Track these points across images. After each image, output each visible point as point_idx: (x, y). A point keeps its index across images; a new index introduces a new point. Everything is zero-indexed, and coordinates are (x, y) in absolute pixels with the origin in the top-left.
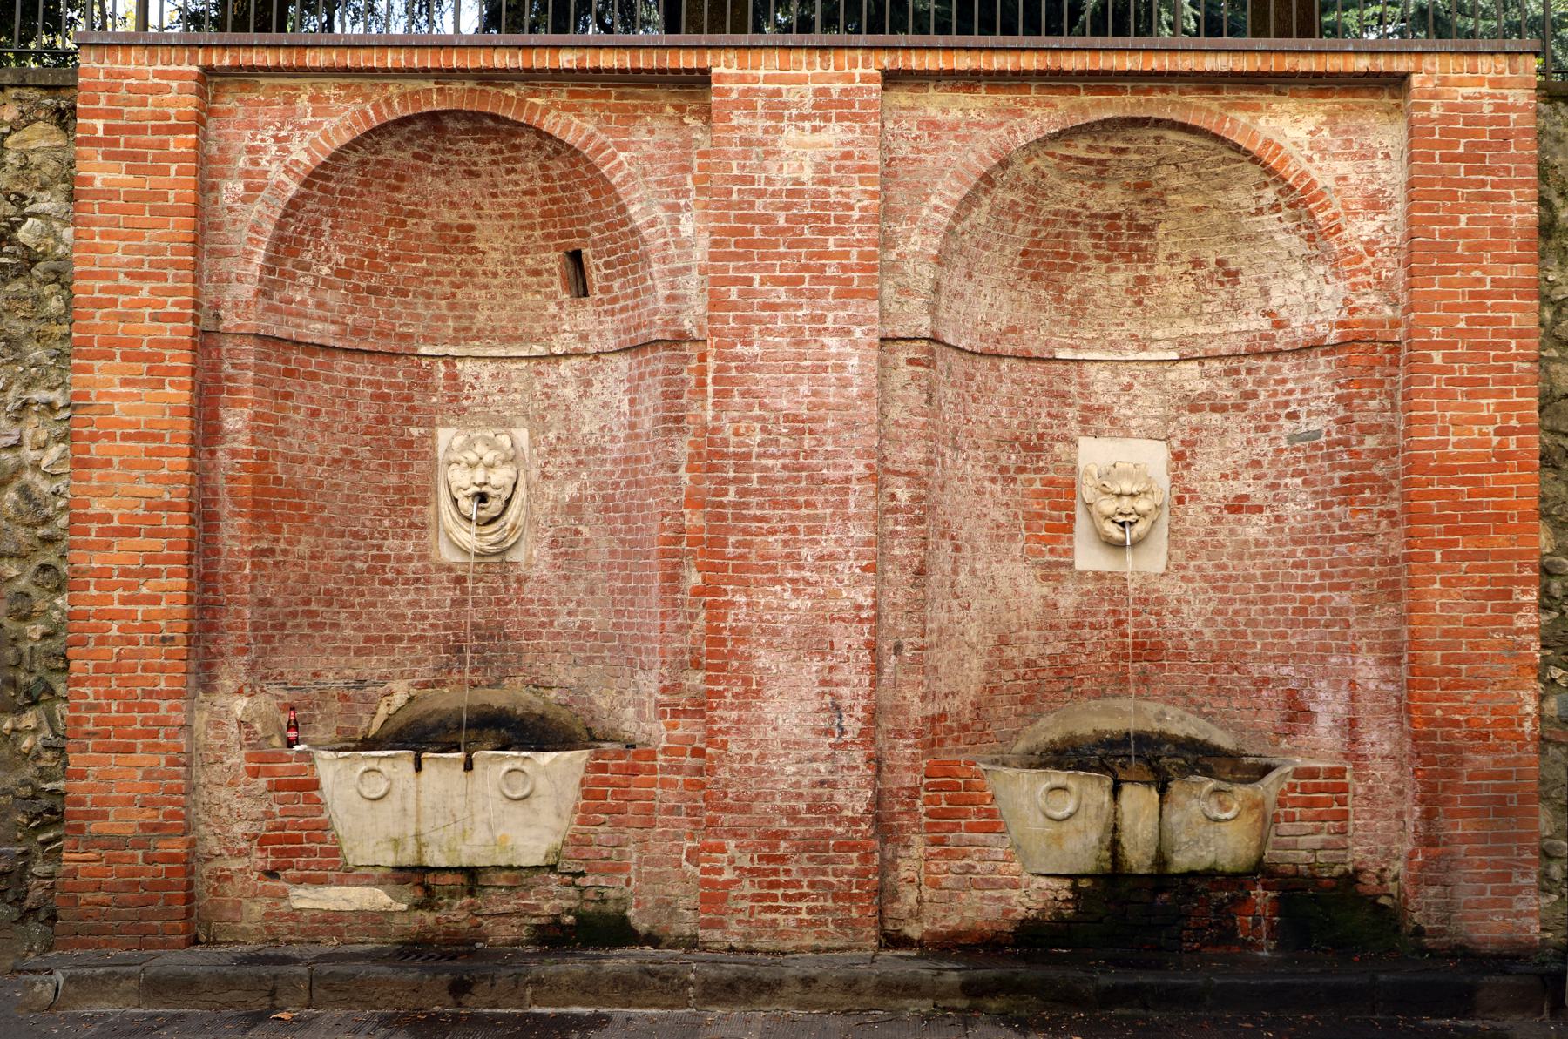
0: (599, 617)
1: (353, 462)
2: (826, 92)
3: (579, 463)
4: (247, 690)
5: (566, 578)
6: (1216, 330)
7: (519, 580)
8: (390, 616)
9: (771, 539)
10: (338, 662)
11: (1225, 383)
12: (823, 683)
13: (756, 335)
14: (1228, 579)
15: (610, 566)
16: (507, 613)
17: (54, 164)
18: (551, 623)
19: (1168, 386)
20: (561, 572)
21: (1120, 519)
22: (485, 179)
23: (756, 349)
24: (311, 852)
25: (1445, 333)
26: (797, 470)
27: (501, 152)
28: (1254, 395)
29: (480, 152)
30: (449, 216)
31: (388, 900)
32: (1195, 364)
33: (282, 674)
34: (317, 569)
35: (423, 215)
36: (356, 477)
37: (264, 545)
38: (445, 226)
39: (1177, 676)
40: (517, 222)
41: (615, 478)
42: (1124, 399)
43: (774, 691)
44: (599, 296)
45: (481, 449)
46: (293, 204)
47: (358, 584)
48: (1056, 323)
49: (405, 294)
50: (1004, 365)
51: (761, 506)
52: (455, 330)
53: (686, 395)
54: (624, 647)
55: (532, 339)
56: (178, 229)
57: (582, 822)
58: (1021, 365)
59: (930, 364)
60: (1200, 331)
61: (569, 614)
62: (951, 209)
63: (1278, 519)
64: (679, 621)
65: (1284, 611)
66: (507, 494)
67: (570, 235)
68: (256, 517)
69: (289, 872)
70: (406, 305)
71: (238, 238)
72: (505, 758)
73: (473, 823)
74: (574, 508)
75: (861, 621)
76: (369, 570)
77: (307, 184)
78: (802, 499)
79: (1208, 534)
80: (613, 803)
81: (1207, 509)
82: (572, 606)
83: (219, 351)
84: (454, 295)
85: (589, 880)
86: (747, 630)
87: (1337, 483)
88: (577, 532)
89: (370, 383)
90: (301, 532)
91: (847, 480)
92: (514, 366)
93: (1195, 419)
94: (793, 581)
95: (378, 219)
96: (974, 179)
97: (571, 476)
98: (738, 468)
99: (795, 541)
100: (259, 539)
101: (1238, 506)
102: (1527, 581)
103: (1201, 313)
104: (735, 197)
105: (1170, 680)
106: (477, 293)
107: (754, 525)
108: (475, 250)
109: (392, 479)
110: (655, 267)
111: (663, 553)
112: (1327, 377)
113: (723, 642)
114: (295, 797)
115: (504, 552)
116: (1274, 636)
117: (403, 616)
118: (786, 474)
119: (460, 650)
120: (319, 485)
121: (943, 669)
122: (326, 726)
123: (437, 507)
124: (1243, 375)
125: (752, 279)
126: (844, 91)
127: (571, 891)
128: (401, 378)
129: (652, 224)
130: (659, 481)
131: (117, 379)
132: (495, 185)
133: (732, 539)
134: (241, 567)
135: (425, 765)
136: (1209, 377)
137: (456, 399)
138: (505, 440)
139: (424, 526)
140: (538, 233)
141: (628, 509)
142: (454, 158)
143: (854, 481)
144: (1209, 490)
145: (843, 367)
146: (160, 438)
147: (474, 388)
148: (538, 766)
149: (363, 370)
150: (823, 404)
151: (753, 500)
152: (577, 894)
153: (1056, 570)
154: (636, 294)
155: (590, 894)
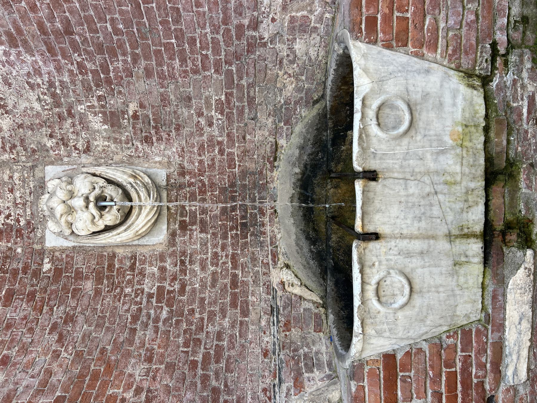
1: (65, 322)
5: (177, 129)
7: (183, 173)
8: (213, 286)
10: (254, 332)
15: (162, 76)
16: (212, 185)
18: (220, 143)
20: (173, 134)
24: (466, 361)
31: (521, 272)
33: (265, 390)
34: (162, 355)
36: (81, 319)
47: (182, 315)
57: (434, 47)
66: (102, 182)
69: (487, 387)
72: (363, 131)
73: (437, 173)
76: (170, 305)
80: (412, 9)
82: (203, 121)
85: (501, 37)
88: (135, 116)
90: (122, 373)
97: (83, 120)
114: (403, 381)
115: (158, 188)
117: (214, 274)
119: (244, 225)
120: (79, 355)
122: (314, 343)
127: (513, 58)
135: (371, 229)
137: (19, 231)
138: (50, 185)
139: (134, 257)
141: (100, 49)
147: (10, 215)
148: (372, 90)
152: (517, 51)
155: (517, 36)
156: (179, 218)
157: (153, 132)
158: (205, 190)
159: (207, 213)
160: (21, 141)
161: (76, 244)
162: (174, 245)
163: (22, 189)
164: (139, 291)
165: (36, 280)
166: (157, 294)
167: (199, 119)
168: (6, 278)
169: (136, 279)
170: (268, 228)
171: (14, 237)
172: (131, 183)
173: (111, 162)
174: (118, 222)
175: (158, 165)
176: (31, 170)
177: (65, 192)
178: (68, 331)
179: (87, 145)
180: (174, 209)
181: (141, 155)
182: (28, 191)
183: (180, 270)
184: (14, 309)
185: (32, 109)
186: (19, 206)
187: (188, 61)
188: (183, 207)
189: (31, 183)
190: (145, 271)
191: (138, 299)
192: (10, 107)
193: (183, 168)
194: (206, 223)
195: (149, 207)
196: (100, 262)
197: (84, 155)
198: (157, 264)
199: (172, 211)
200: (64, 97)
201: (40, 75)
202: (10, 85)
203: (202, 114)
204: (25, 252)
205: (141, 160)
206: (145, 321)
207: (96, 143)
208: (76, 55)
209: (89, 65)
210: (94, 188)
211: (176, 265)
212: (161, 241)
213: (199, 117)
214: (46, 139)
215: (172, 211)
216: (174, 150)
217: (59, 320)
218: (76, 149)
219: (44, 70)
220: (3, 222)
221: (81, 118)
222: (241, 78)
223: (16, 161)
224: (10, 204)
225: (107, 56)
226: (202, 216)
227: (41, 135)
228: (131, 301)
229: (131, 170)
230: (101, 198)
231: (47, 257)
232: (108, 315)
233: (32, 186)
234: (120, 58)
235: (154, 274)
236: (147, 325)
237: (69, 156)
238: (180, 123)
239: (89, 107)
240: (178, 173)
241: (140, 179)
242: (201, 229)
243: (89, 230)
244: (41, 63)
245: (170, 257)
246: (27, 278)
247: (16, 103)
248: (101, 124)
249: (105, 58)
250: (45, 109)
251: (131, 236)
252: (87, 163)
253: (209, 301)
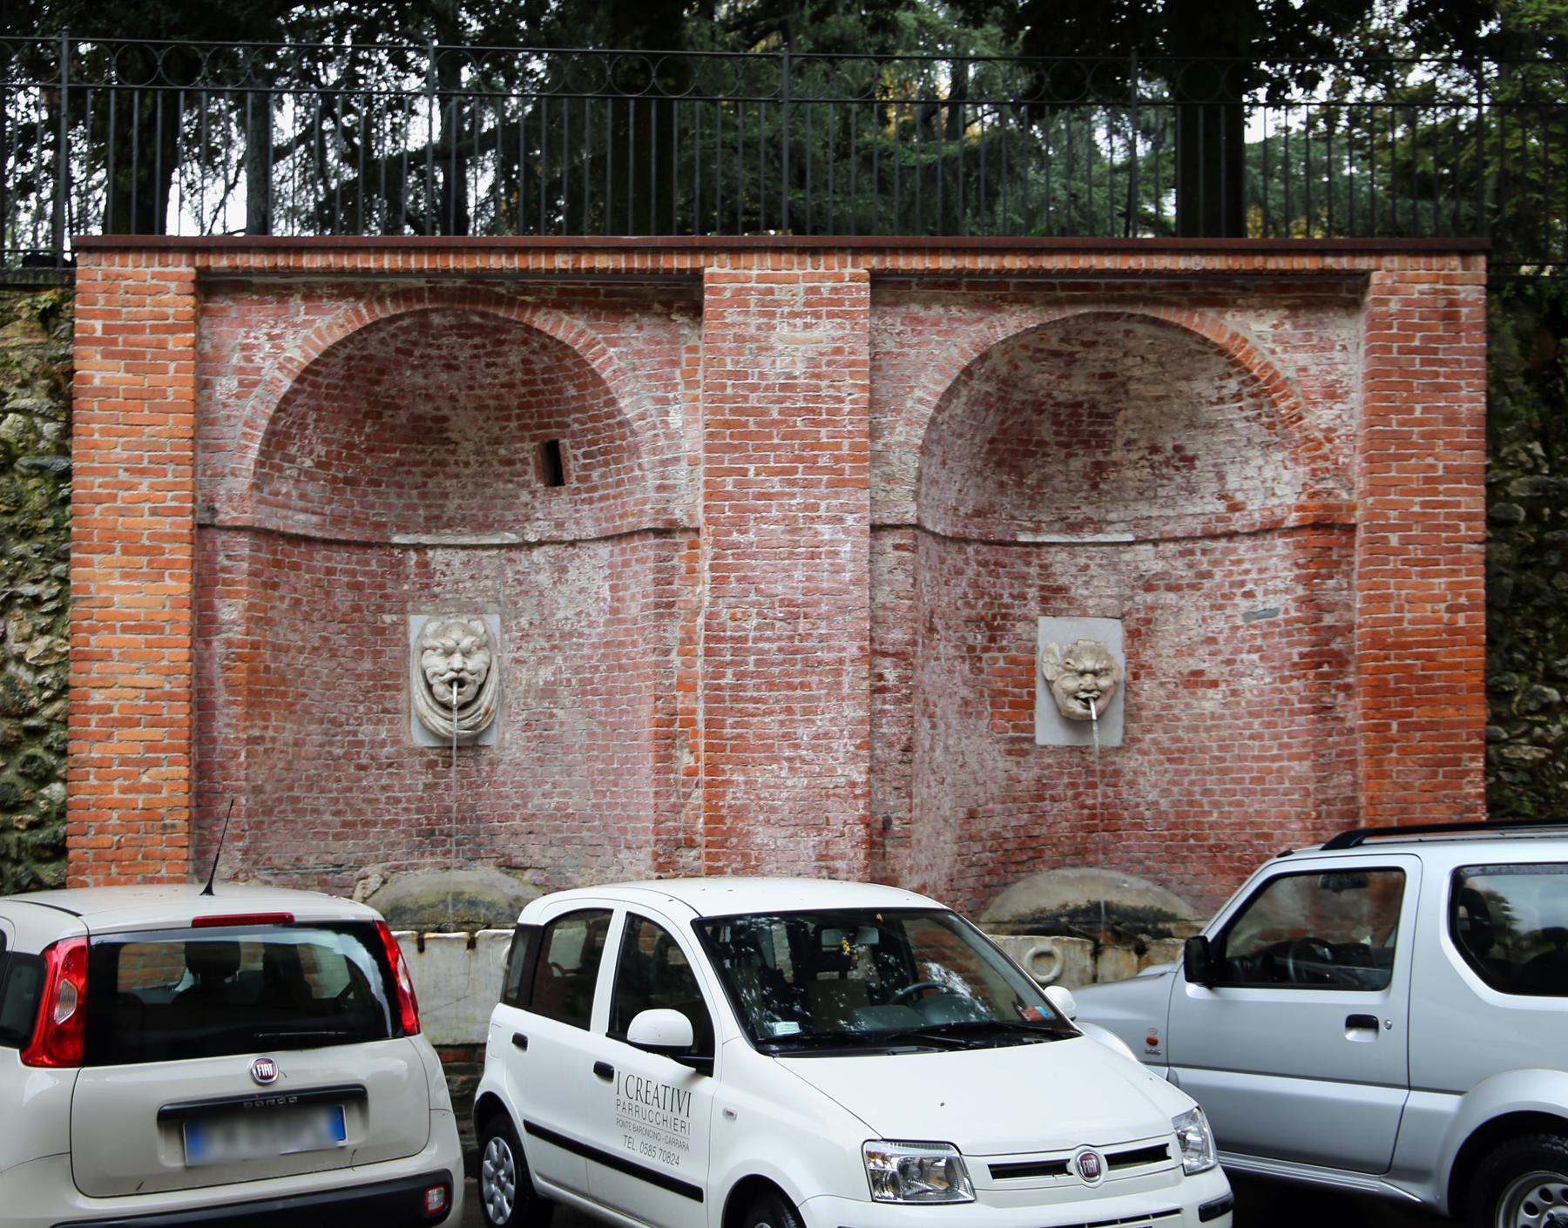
0: (576, 799)
2: (814, 291)
3: (554, 647)
4: (242, 876)
6: (1170, 512)
7: (491, 763)
8: (364, 800)
9: (767, 720)
11: (1180, 563)
12: (821, 857)
13: (752, 523)
14: (1185, 751)
15: (590, 748)
17: (34, 361)
18: (525, 806)
19: (1123, 568)
21: (1083, 695)
22: (464, 372)
23: (751, 537)
25: (1402, 516)
26: (793, 653)
27: (484, 346)
28: (1208, 575)
29: (462, 346)
30: (424, 408)
32: (1150, 547)
35: (399, 407)
36: (333, 664)
37: (256, 732)
38: (420, 418)
39: (1133, 842)
40: (493, 414)
41: (593, 662)
42: (1080, 581)
43: (773, 866)
44: (575, 485)
45: (456, 634)
46: (286, 400)
47: (336, 770)
48: (1017, 507)
49: (377, 483)
50: (970, 550)
51: (757, 688)
52: (427, 519)
53: (677, 582)
54: (605, 827)
55: (504, 526)
56: (179, 424)
58: (984, 549)
59: (914, 549)
60: (1155, 513)
61: (544, 795)
62: (935, 401)
63: (1234, 693)
64: (673, 800)
65: (1241, 781)
66: (480, 680)
67: (548, 426)
68: (251, 705)
70: (378, 494)
71: (232, 433)
74: (548, 692)
75: (856, 797)
76: (346, 756)
77: (300, 380)
78: (798, 680)
79: (1163, 709)
81: (1162, 684)
82: (547, 787)
83: (214, 544)
84: (425, 484)
86: (745, 807)
87: (1296, 659)
88: (552, 716)
89: (346, 572)
91: (841, 661)
92: (486, 553)
93: (1150, 598)
94: (790, 759)
95: (357, 411)
96: (956, 372)
97: (547, 660)
98: (735, 652)
99: (792, 721)
100: (252, 727)
101: (1195, 680)
102: (1474, 749)
103: (1156, 497)
104: (729, 391)
105: (1128, 849)
106: (448, 483)
107: (751, 706)
108: (448, 441)
109: (366, 665)
110: (646, 459)
111: (657, 736)
112: (1284, 558)
113: (721, 820)
116: (1230, 804)
117: (377, 800)
118: (781, 657)
119: (432, 833)
120: (301, 673)
121: (924, 842)
123: (409, 693)
124: (1198, 556)
125: (747, 470)
126: (835, 290)
128: (374, 566)
129: (642, 417)
130: (650, 665)
131: (117, 572)
132: (473, 378)
133: (730, 721)
134: (236, 755)
135: (427, 945)
136: (1164, 558)
137: (427, 586)
138: (477, 626)
140: (513, 424)
141: (610, 693)
142: (434, 352)
143: (848, 663)
144: (1165, 666)
145: (836, 553)
146: (160, 630)
149: (340, 559)
150: (817, 589)
151: (750, 682)
153: (1020, 746)
154: (619, 483)
170: (429, 860)
192: (563, 588)
219: (594, 632)
222: (589, 830)
223: (505, 583)
230: (461, 683)
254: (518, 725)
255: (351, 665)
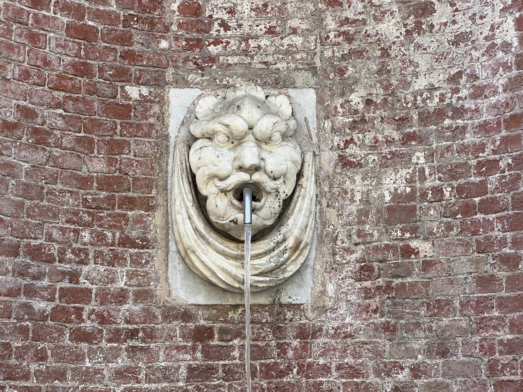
1: (36, 131)
5: (387, 328)
36: (40, 157)
41: (486, 155)
47: (37, 338)
66: (286, 190)
76: (56, 314)
88: (408, 252)
123: (167, 214)
137: (199, 43)
147: (227, 28)
156: (217, 325)
157: (381, 282)
158: (272, 377)
159: (226, 381)
160: (359, 52)
161: (172, 140)
162: (166, 317)
163: (274, 48)
164: (83, 256)
165: (110, 75)
166: (76, 289)
167: (407, 370)
168: (116, 26)
169: (105, 250)
171: (188, 36)
172: (284, 240)
173: (325, 204)
174: (213, 218)
175: (319, 288)
176: (307, 64)
177: (268, 132)
178: (20, 138)
179: (354, 163)
180: (236, 317)
181: (338, 258)
182: (270, 59)
183: (118, 331)
184: (63, 43)
185: (416, 75)
186: (244, 44)
187: (511, 357)
188: (239, 334)
189: (285, 65)
190: (120, 265)
191: (69, 255)
192: (418, 39)
193: (314, 336)
194: (208, 378)
195: (239, 273)
196: (138, 183)
197: (335, 155)
198: (132, 286)
199: (231, 314)
200: (437, 130)
201: (474, 96)
202: (455, 43)
203: (416, 377)
204: (160, 55)
205: (329, 259)
206: (30, 271)
207: (358, 178)
208: (510, 161)
209: (493, 179)
210: (275, 179)
211: (128, 322)
212: (174, 293)
213: (412, 370)
214: (363, 93)
215: (231, 314)
216: (348, 320)
217: (39, 120)
218: (347, 143)
219: (483, 104)
220: (215, 17)
221: (401, 156)
223: (324, 40)
224: (246, 29)
225: (511, 212)
226: (220, 371)
227: (371, 86)
228: (66, 244)
229: (309, 241)
231: (150, 92)
232: (45, 203)
233: (279, 65)
234: (509, 235)
235: (113, 281)
236: (22, 274)
237: (334, 130)
238: (398, 333)
239: (422, 171)
240: (304, 325)
241: (293, 258)
242: (195, 369)
243: (199, 168)
244: (493, 100)
245: (144, 310)
246: (115, 60)
247: (425, 49)
248: (392, 190)
249: (506, 209)
250: (415, 97)
251: (186, 240)
252: (322, 161)
253: (57, 388)
254: (348, 270)
255: (71, 161)
